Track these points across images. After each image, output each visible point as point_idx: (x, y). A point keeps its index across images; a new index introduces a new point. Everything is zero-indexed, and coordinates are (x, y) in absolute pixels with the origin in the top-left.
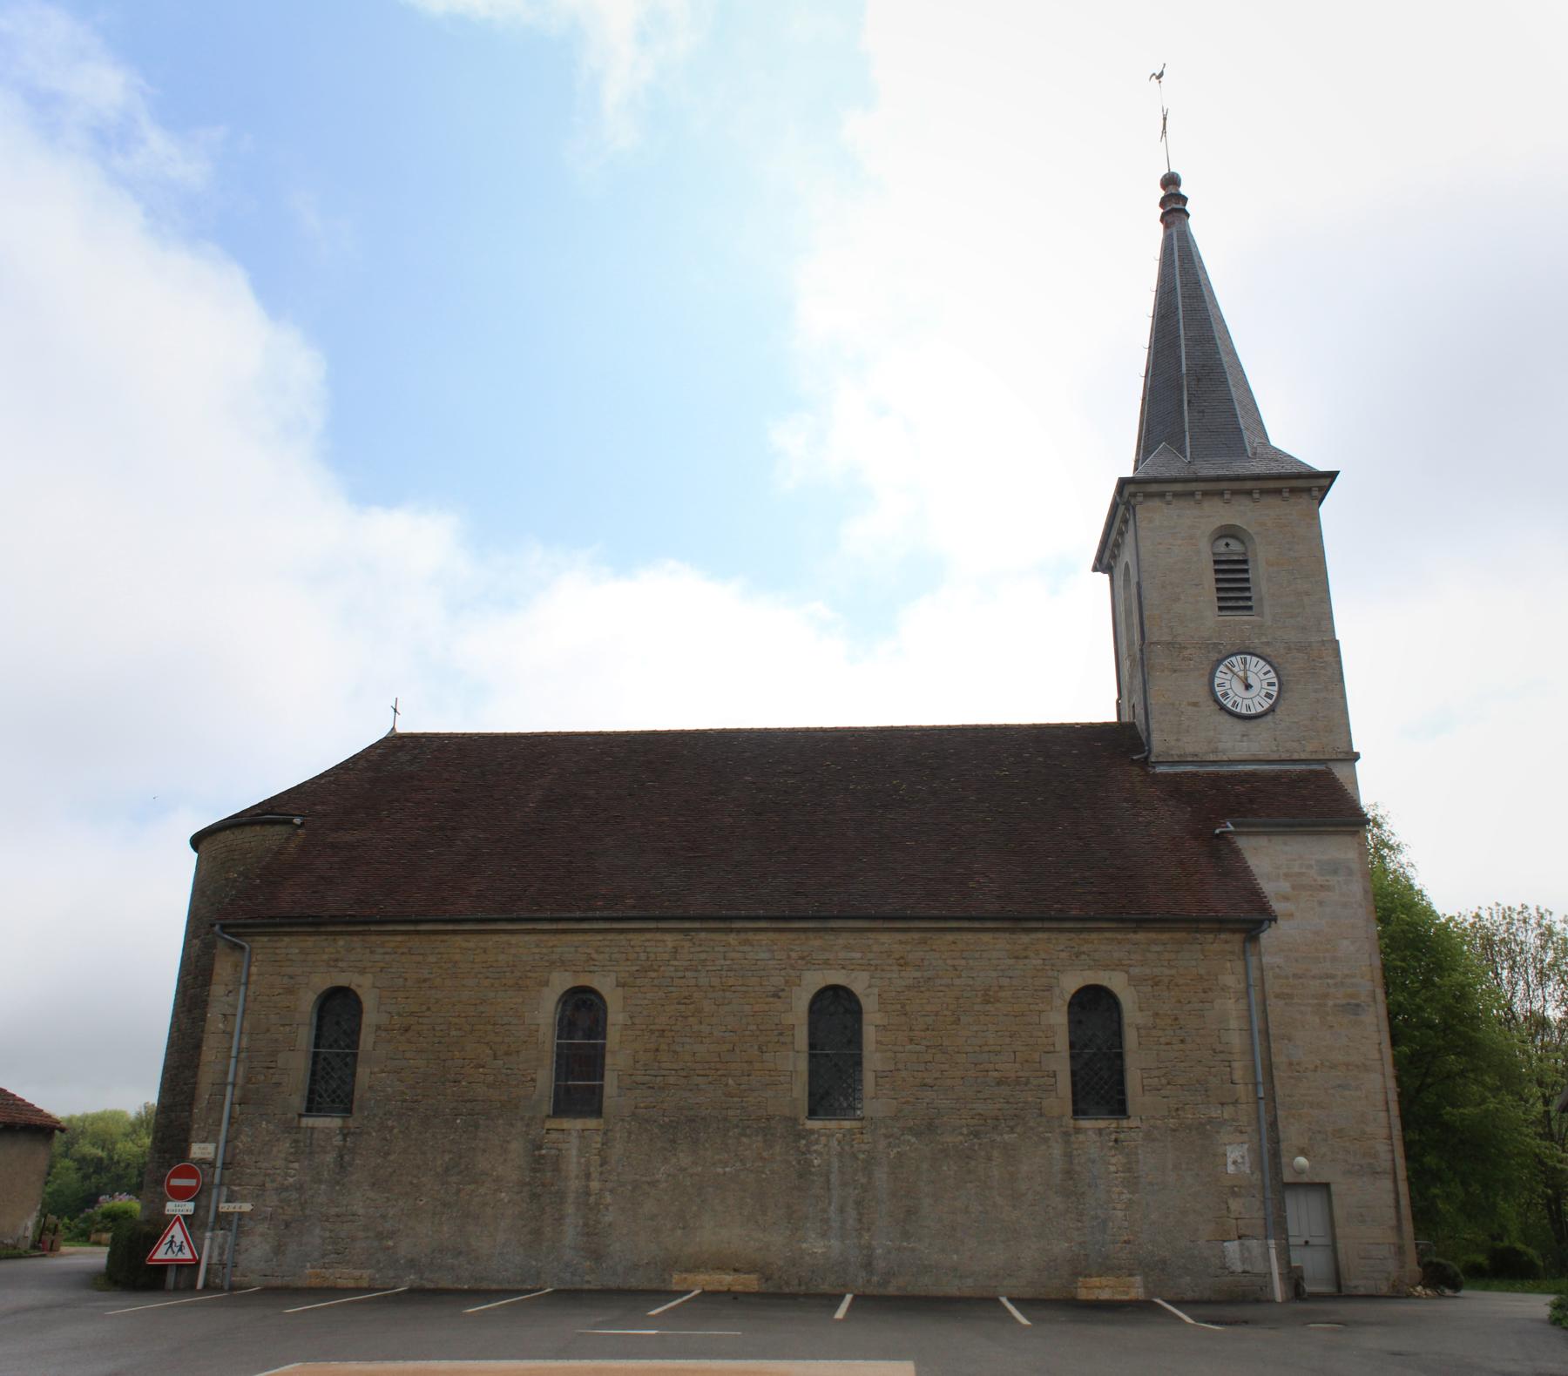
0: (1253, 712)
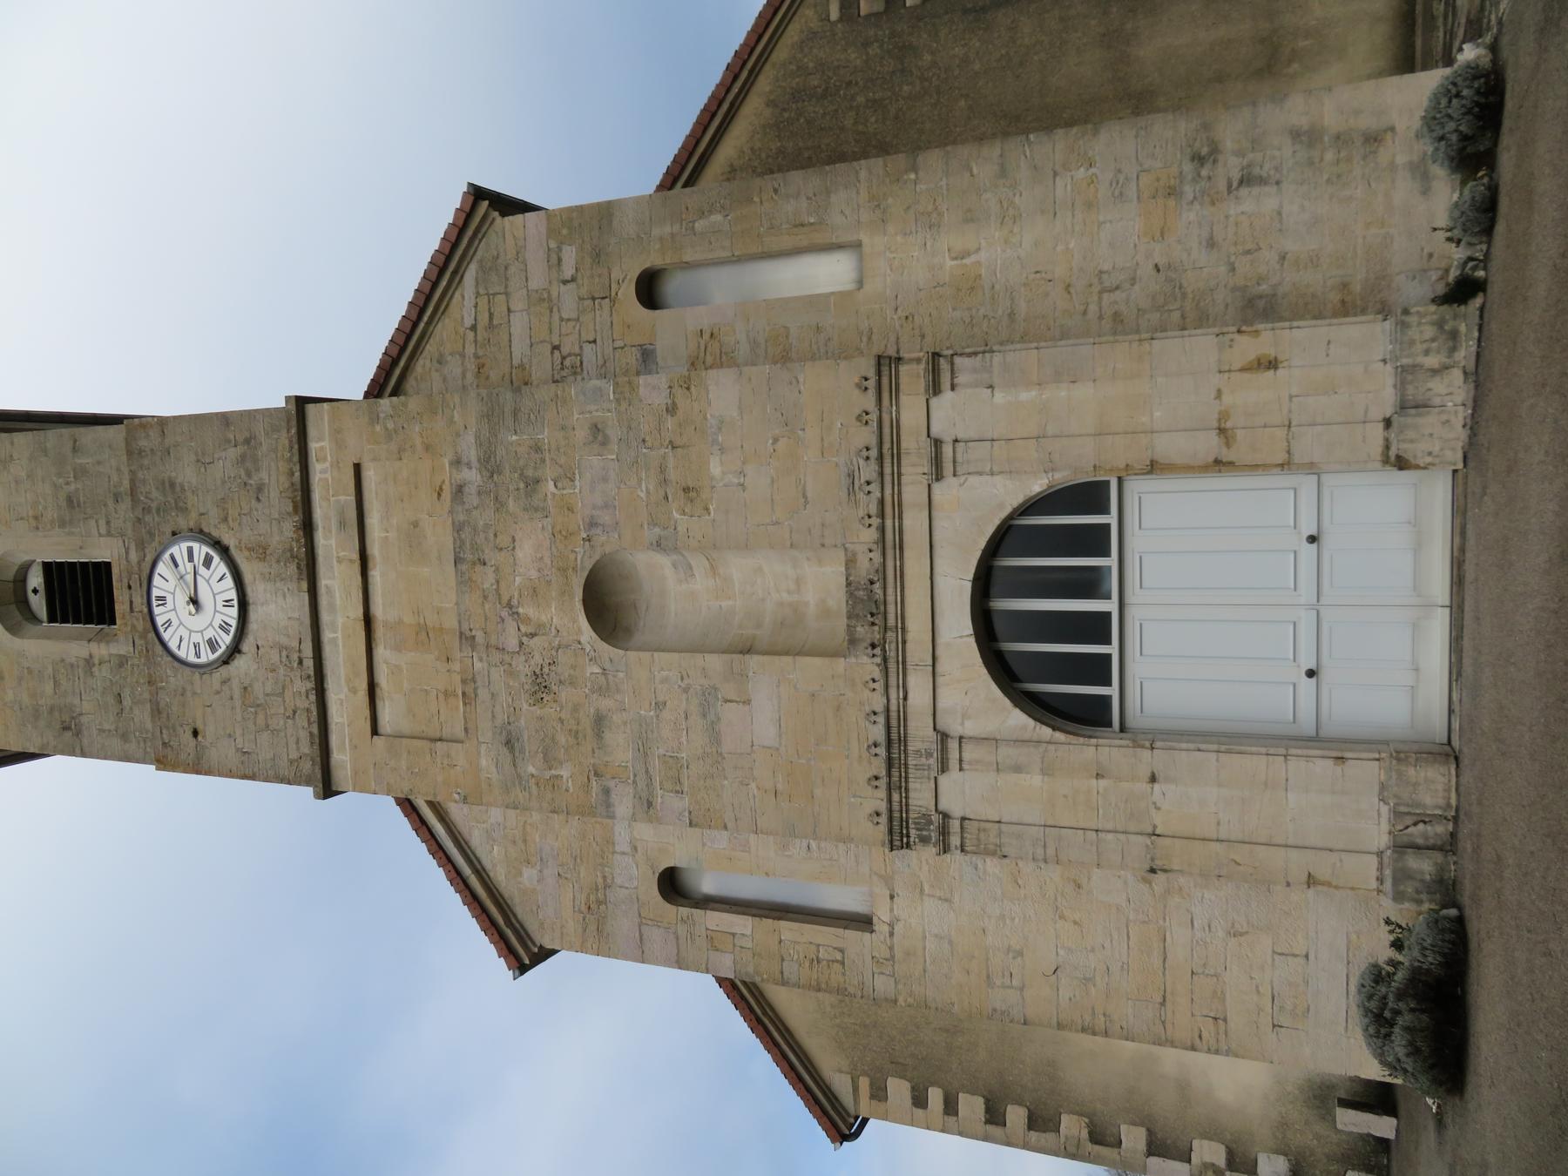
0: (233, 595)
